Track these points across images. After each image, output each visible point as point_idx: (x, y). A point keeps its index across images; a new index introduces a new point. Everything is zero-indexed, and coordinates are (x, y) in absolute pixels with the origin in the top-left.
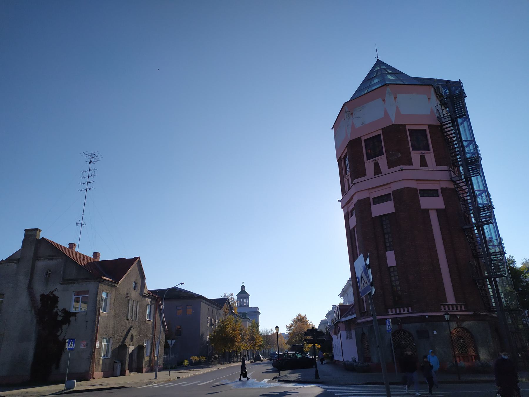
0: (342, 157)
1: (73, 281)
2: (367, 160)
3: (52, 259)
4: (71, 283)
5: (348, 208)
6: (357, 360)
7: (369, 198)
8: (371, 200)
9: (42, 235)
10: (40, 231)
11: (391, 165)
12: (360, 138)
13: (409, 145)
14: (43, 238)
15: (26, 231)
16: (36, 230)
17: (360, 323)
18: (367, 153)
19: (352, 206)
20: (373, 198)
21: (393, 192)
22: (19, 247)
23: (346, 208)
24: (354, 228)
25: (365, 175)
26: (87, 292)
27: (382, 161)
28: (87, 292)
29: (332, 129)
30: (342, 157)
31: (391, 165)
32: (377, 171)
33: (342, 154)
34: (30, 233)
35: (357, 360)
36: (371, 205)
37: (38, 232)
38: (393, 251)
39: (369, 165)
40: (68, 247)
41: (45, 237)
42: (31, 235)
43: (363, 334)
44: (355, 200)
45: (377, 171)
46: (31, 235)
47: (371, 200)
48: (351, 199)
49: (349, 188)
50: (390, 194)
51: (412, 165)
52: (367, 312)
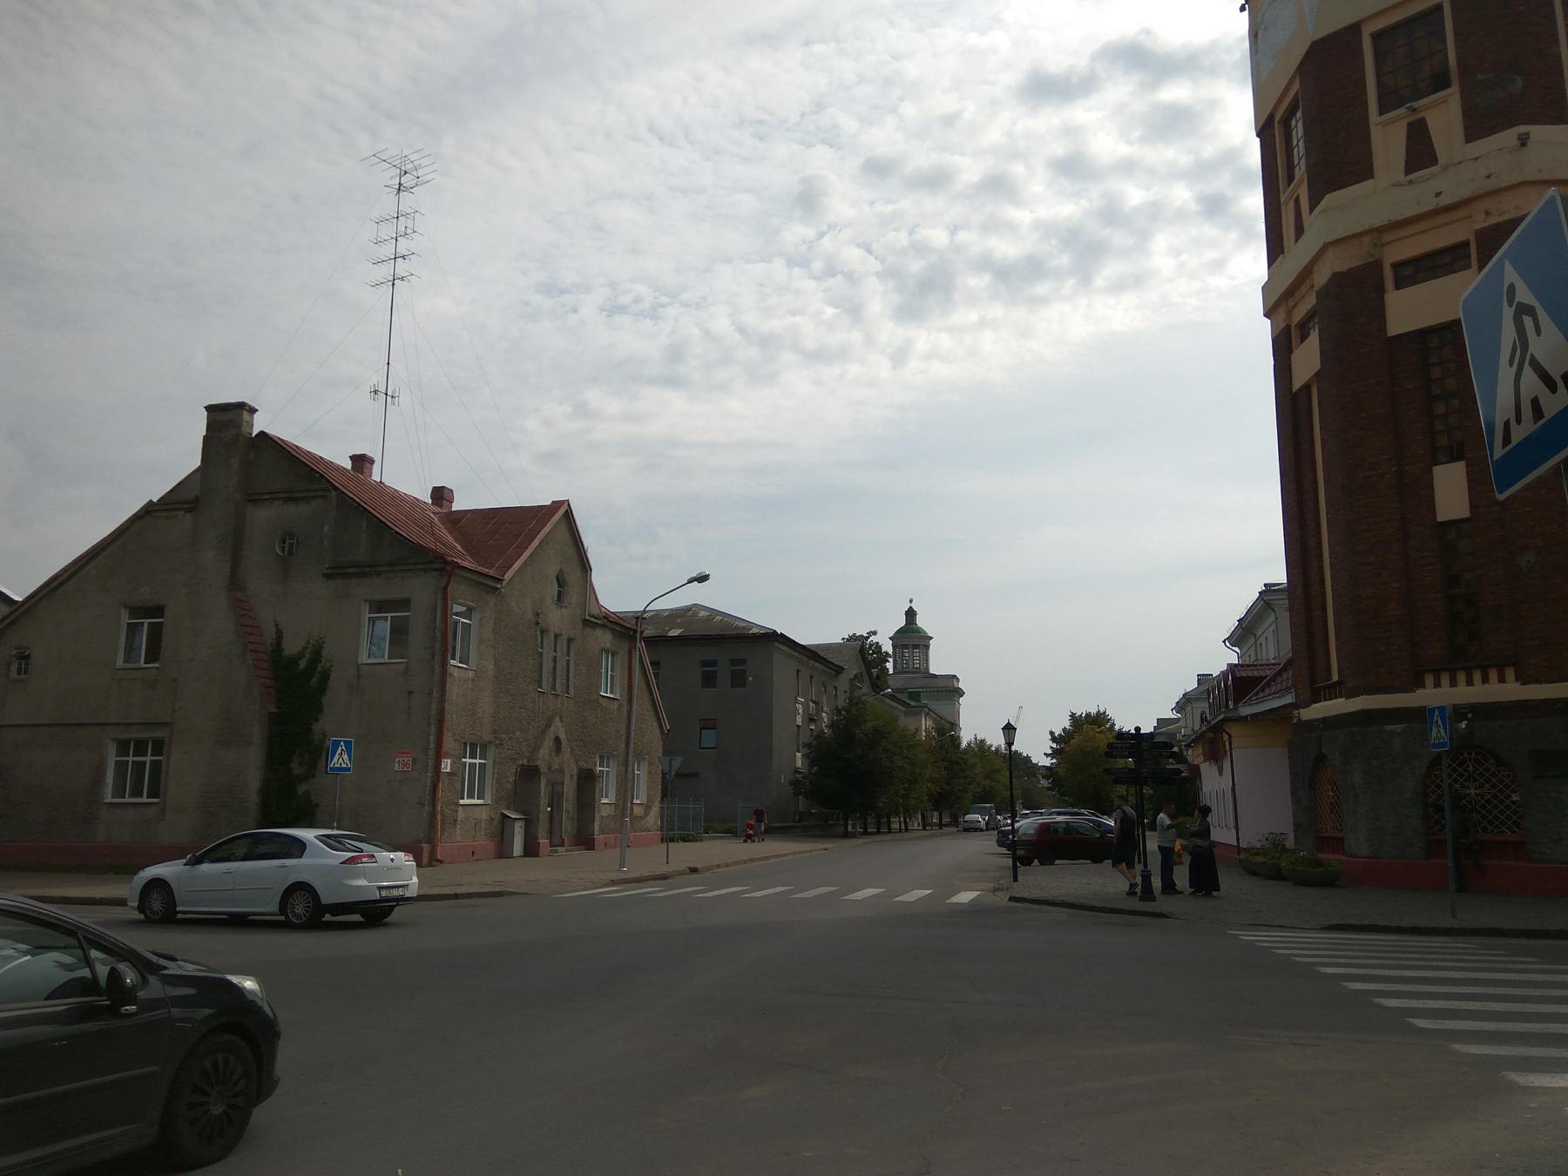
1: (363, 570)
2: (1381, 114)
3: (296, 500)
5: (1289, 313)
6: (1290, 843)
8: (1388, 273)
9: (260, 424)
10: (253, 411)
11: (1478, 125)
12: (1354, 29)
14: (262, 433)
15: (211, 409)
16: (241, 406)
17: (1310, 724)
18: (1380, 85)
20: (1396, 266)
21: (1480, 234)
22: (195, 462)
24: (1307, 387)
26: (404, 604)
27: (1444, 115)
28: (404, 604)
29: (1242, 9)
30: (1277, 119)
31: (1478, 125)
32: (1420, 153)
33: (1279, 102)
34: (220, 416)
35: (1290, 843)
36: (1382, 290)
37: (245, 414)
39: (1387, 140)
40: (348, 465)
42: (226, 421)
43: (1321, 759)
44: (1321, 277)
45: (1420, 153)
46: (226, 421)
47: (1388, 273)
48: (1307, 273)
50: (1466, 244)
52: (1339, 683)
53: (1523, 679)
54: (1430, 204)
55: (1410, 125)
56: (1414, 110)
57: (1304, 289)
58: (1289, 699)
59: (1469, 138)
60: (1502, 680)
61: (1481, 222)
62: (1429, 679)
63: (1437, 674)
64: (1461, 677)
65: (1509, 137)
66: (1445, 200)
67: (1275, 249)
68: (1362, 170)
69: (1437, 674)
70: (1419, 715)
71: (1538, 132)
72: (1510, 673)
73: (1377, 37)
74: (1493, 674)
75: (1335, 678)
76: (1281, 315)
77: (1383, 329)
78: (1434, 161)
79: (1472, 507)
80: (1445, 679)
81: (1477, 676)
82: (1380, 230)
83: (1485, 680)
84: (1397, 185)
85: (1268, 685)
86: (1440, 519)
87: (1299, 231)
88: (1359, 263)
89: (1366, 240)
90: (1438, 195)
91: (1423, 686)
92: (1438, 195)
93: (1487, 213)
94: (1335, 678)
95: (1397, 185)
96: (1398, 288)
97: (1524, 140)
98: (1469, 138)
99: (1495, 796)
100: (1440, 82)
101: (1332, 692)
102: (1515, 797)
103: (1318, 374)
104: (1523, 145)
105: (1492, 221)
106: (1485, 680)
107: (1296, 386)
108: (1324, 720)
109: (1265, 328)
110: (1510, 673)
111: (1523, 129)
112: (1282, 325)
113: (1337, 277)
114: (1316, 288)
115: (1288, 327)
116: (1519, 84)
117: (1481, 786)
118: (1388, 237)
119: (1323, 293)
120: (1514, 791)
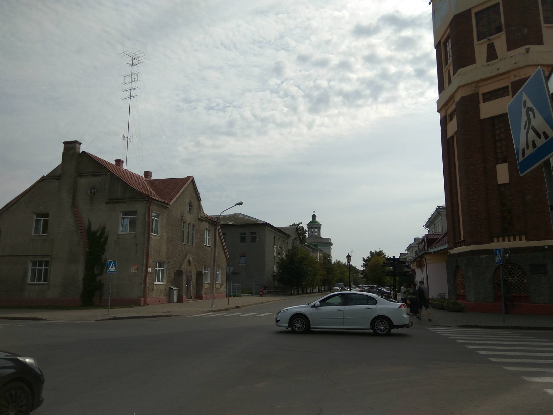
0: (442, 42)
2: (478, 41)
3: (95, 176)
4: (117, 202)
5: (446, 111)
6: (447, 297)
7: (477, 94)
8: (481, 97)
9: (83, 148)
10: (80, 144)
11: (511, 45)
12: (469, 11)
13: (539, 16)
14: (83, 152)
16: (76, 142)
17: (454, 255)
19: (453, 107)
21: (513, 83)
22: (60, 162)
23: (443, 111)
24: (452, 137)
25: (473, 62)
26: (134, 213)
27: (500, 42)
28: (134, 213)
29: (430, 4)
30: (442, 42)
31: (511, 45)
32: (492, 55)
34: (68, 146)
35: (447, 297)
36: (479, 103)
37: (77, 145)
38: (506, 164)
39: (480, 50)
40: (114, 163)
41: (86, 151)
42: (71, 148)
44: (457, 98)
45: (492, 55)
46: (71, 148)
47: (481, 97)
48: (452, 97)
49: (450, 82)
50: (508, 87)
51: (543, 44)
52: (464, 241)
53: (528, 239)
54: (495, 73)
55: (488, 45)
56: (490, 40)
57: (451, 102)
58: (446, 246)
59: (509, 49)
60: (520, 240)
61: (513, 79)
62: (495, 239)
63: (498, 237)
64: (506, 239)
65: (522, 49)
66: (500, 71)
67: (441, 88)
68: (472, 60)
69: (498, 237)
70: (491, 252)
71: (533, 48)
72: (523, 237)
73: (476, 14)
74: (518, 238)
75: (462, 239)
76: (443, 111)
77: (479, 116)
78: (496, 57)
79: (510, 179)
80: (501, 239)
81: (512, 238)
82: (478, 82)
83: (515, 240)
84: (484, 66)
85: (439, 241)
86: (499, 183)
87: (450, 82)
88: (471, 93)
89: (473, 85)
90: (498, 69)
91: (493, 242)
92: (498, 69)
93: (515, 76)
94: (462, 239)
95: (484, 66)
96: (484, 102)
97: (528, 51)
98: (509, 49)
99: (518, 280)
100: (499, 30)
101: (461, 244)
102: (525, 281)
103: (456, 132)
104: (528, 52)
105: (517, 79)
106: (515, 240)
107: (449, 136)
108: (459, 254)
109: (437, 116)
110: (523, 237)
111: (527, 46)
112: (444, 115)
113: (463, 98)
114: (456, 102)
115: (446, 116)
116: (526, 31)
117: (514, 277)
118: (480, 84)
119: (458, 104)
120: (525, 279)
